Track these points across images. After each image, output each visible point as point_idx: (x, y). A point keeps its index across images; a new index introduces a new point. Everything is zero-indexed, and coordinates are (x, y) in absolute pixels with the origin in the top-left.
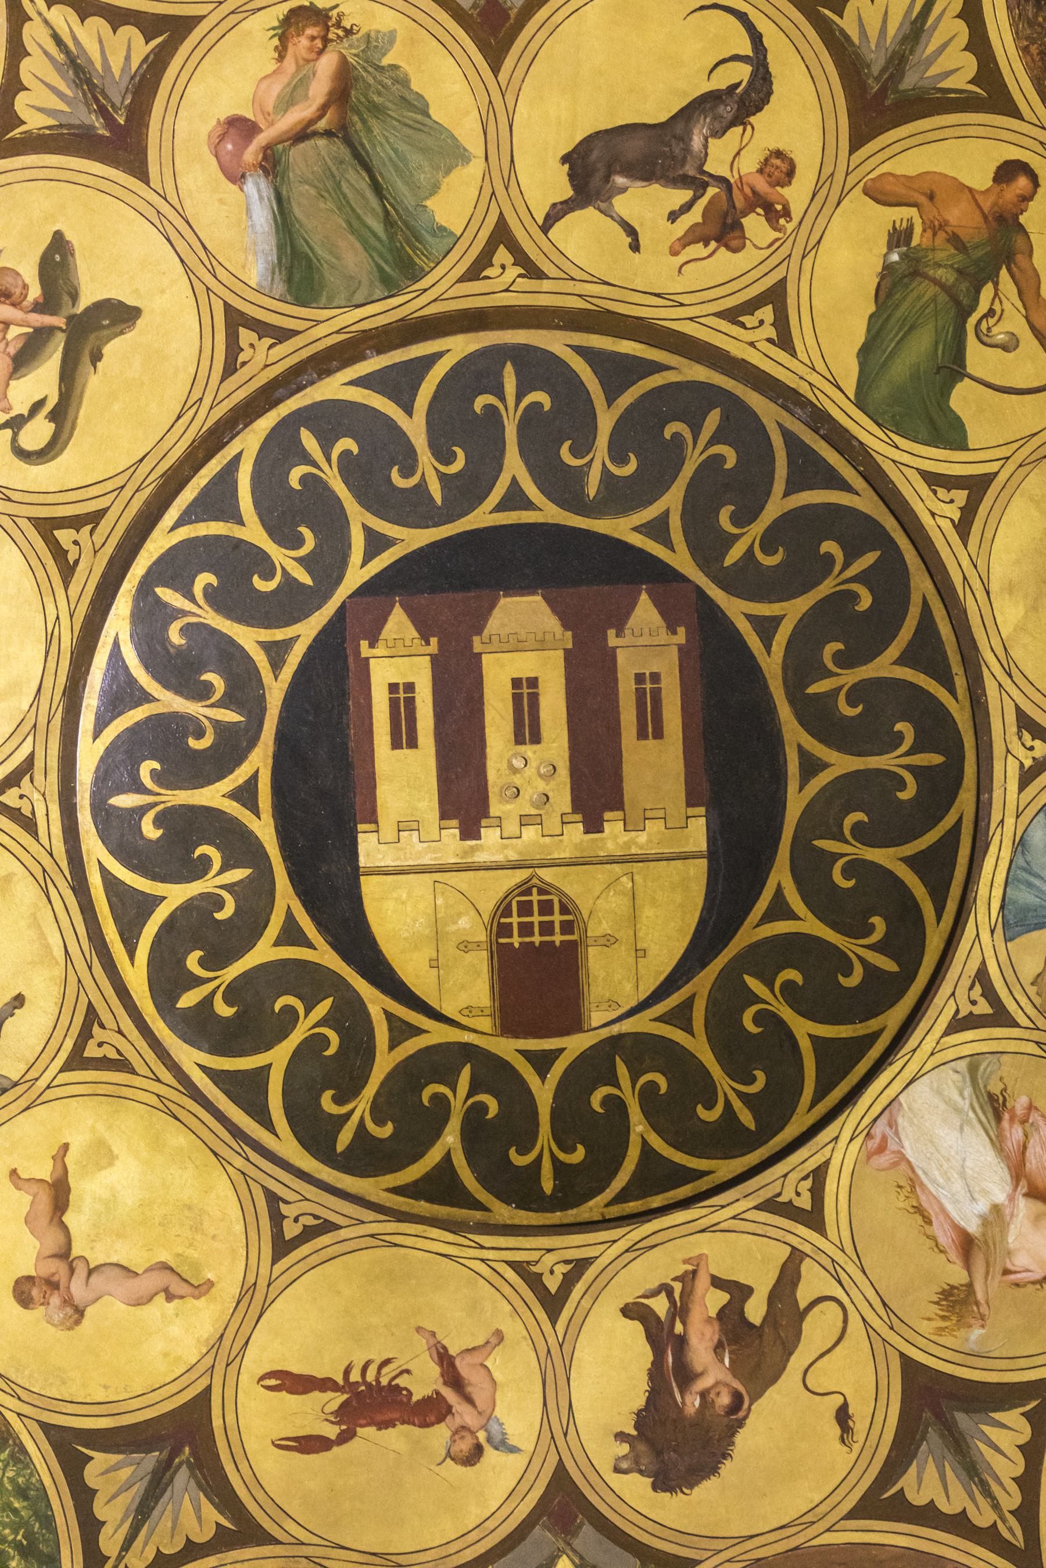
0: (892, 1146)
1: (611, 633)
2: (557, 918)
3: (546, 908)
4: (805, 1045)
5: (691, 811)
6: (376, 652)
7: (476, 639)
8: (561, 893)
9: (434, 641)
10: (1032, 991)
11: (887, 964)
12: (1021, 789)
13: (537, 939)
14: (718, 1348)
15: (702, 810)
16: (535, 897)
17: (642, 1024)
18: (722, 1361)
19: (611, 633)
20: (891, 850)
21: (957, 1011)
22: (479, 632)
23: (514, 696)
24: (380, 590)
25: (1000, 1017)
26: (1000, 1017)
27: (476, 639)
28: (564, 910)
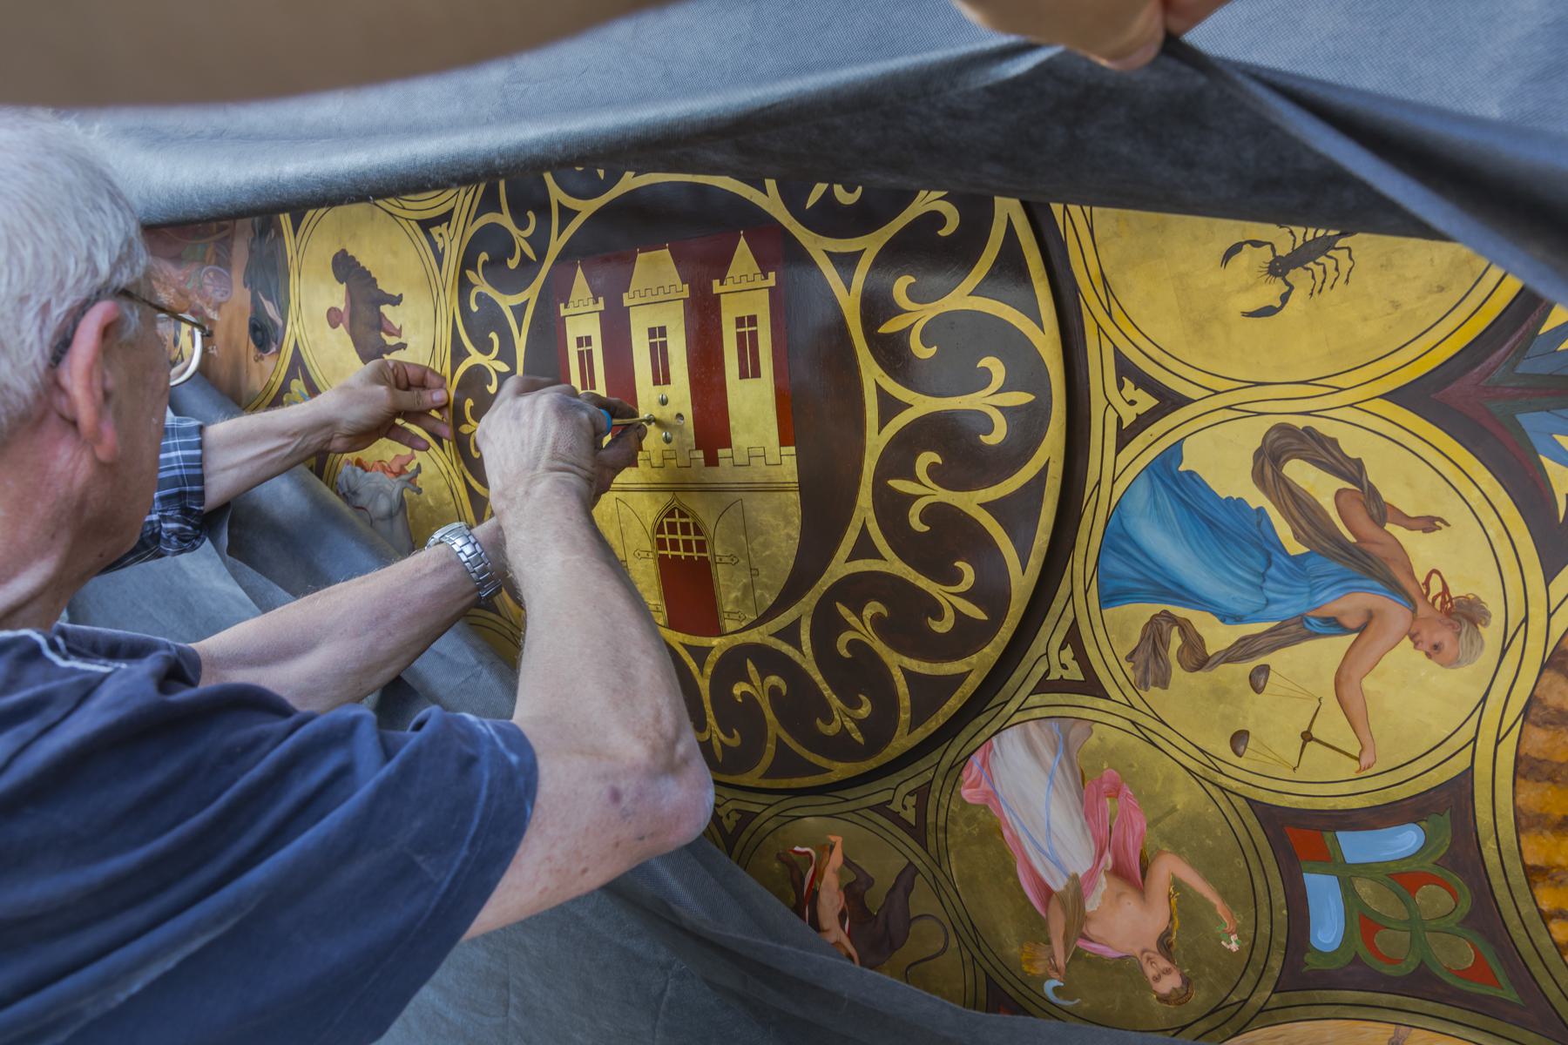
0: (985, 785)
1: (716, 283)
2: (692, 537)
3: (685, 529)
4: (898, 676)
5: (785, 450)
6: (571, 310)
7: (625, 295)
8: (695, 516)
9: (601, 299)
10: (1127, 667)
11: (977, 613)
12: (1121, 446)
13: (682, 553)
14: (842, 916)
15: (792, 449)
16: (677, 519)
17: (754, 636)
18: (843, 927)
19: (716, 283)
20: (871, 514)
21: (1048, 672)
22: (627, 290)
23: (653, 346)
24: (566, 255)
25: (1091, 686)
26: (1091, 686)
27: (625, 295)
28: (698, 532)
